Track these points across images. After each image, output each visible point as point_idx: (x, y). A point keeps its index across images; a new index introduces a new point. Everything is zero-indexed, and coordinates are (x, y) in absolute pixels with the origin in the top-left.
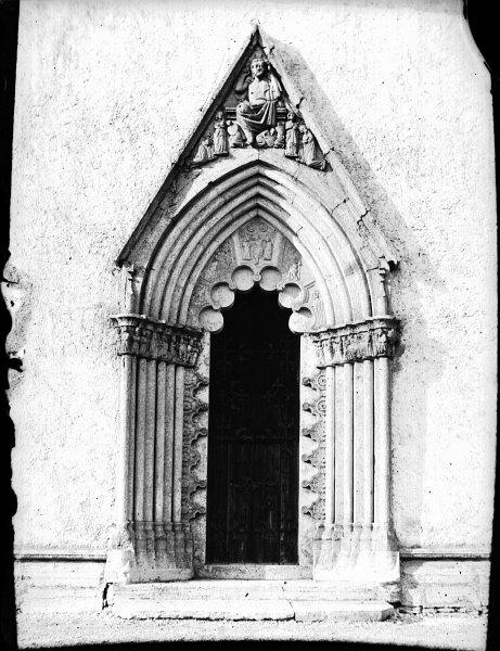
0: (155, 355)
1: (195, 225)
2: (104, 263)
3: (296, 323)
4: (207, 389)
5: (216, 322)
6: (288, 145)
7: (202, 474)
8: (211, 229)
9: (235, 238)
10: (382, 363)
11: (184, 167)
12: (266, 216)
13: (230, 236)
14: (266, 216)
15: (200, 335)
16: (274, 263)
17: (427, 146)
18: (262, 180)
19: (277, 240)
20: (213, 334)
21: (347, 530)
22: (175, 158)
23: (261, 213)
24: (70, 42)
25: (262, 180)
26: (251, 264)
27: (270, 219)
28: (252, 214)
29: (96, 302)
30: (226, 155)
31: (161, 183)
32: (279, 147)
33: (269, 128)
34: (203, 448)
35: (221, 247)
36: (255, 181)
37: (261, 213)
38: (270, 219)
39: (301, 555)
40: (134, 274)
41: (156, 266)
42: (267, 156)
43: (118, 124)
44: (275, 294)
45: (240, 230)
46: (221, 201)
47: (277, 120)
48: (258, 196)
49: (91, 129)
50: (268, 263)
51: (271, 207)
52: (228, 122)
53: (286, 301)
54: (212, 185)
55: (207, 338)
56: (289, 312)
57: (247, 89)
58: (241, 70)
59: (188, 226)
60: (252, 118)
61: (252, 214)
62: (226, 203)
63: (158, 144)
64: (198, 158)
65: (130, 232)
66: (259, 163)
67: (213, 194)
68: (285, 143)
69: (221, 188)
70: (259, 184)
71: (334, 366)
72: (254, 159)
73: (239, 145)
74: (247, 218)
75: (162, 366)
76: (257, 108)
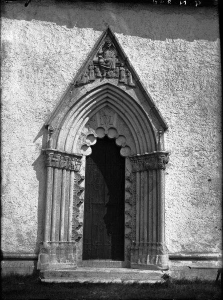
1: (80, 109)
3: (123, 152)
5: (89, 151)
7: (81, 220)
9: (97, 115)
15: (80, 157)
16: (114, 126)
18: (109, 91)
19: (116, 116)
20: (87, 157)
21: (146, 245)
23: (109, 105)
25: (109, 91)
26: (104, 126)
27: (112, 107)
28: (105, 105)
30: (92, 81)
33: (113, 69)
34: (81, 209)
36: (106, 91)
37: (109, 105)
38: (112, 107)
39: (125, 257)
42: (111, 81)
44: (114, 140)
45: (99, 111)
47: (116, 66)
49: (35, 68)
50: (111, 126)
53: (118, 143)
54: (88, 93)
55: (84, 159)
56: (120, 147)
59: (77, 110)
61: (105, 105)
66: (108, 84)
67: (88, 97)
69: (91, 94)
70: (108, 93)
71: (140, 172)
72: (106, 83)
73: (98, 77)
74: (102, 106)
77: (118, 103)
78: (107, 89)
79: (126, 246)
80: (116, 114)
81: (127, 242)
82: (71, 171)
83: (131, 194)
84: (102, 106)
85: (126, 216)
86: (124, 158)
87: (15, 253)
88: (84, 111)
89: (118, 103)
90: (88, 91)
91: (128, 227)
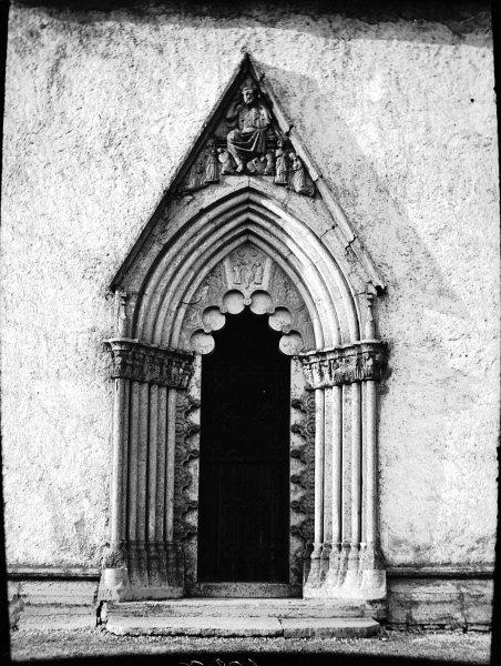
0: (147, 379)
1: (186, 250)
2: (97, 288)
4: (199, 411)
5: (207, 345)
6: (278, 172)
7: (194, 496)
8: (202, 254)
9: (226, 263)
10: (369, 387)
11: (175, 193)
12: (256, 241)
13: (221, 261)
14: (256, 241)
15: (190, 358)
16: (264, 287)
17: (415, 172)
18: (252, 207)
19: (268, 265)
21: (335, 549)
22: (167, 184)
23: (252, 238)
24: (63, 70)
25: (252, 207)
26: (242, 288)
27: (261, 244)
28: (243, 239)
29: (90, 326)
30: (216, 182)
31: (153, 210)
32: (269, 174)
34: (194, 469)
35: (212, 271)
37: (252, 238)
38: (261, 244)
39: (292, 575)
40: (127, 299)
41: (149, 291)
43: (112, 151)
44: (266, 317)
45: (230, 255)
46: (212, 226)
47: (267, 148)
48: (249, 221)
49: (84, 157)
50: (258, 287)
51: (261, 233)
52: (219, 150)
53: (275, 324)
55: (198, 360)
56: (280, 335)
57: (238, 115)
58: (231, 97)
59: (179, 252)
60: (242, 146)
61: (243, 239)
62: (217, 229)
63: (151, 171)
64: (191, 185)
65: (123, 257)
66: (249, 189)
67: (204, 220)
68: (275, 171)
69: (211, 214)
70: (249, 210)
71: (323, 389)
72: (244, 186)
74: (237, 243)
75: (155, 389)
76: (248, 135)
77: (272, 234)
78: (248, 201)
79: (292, 553)
80: (268, 259)
81: (295, 544)
82: (168, 389)
83: (304, 437)
84: (237, 243)
85: (292, 487)
86: (287, 359)
87: (50, 566)
88: (196, 254)
89: (272, 234)
90: (204, 206)
91: (298, 510)
